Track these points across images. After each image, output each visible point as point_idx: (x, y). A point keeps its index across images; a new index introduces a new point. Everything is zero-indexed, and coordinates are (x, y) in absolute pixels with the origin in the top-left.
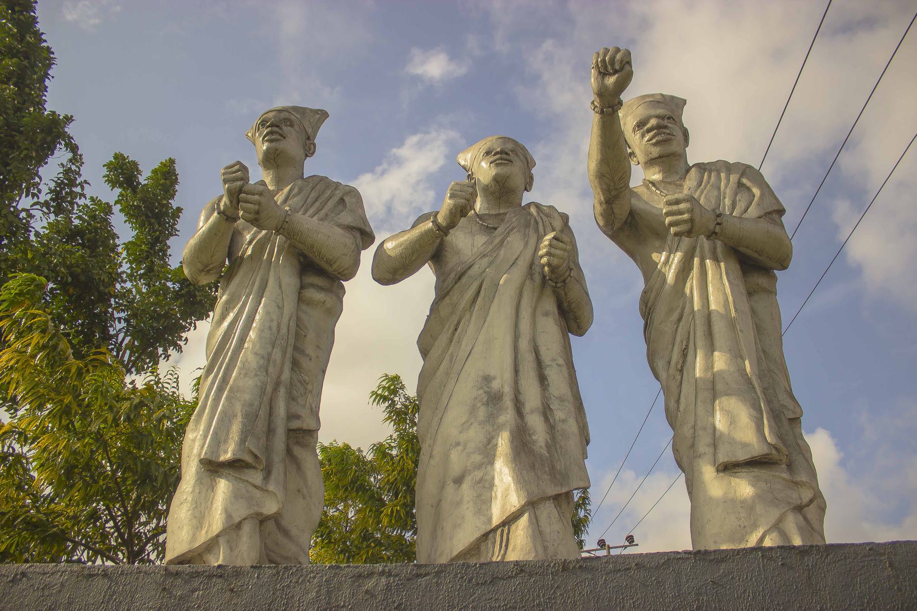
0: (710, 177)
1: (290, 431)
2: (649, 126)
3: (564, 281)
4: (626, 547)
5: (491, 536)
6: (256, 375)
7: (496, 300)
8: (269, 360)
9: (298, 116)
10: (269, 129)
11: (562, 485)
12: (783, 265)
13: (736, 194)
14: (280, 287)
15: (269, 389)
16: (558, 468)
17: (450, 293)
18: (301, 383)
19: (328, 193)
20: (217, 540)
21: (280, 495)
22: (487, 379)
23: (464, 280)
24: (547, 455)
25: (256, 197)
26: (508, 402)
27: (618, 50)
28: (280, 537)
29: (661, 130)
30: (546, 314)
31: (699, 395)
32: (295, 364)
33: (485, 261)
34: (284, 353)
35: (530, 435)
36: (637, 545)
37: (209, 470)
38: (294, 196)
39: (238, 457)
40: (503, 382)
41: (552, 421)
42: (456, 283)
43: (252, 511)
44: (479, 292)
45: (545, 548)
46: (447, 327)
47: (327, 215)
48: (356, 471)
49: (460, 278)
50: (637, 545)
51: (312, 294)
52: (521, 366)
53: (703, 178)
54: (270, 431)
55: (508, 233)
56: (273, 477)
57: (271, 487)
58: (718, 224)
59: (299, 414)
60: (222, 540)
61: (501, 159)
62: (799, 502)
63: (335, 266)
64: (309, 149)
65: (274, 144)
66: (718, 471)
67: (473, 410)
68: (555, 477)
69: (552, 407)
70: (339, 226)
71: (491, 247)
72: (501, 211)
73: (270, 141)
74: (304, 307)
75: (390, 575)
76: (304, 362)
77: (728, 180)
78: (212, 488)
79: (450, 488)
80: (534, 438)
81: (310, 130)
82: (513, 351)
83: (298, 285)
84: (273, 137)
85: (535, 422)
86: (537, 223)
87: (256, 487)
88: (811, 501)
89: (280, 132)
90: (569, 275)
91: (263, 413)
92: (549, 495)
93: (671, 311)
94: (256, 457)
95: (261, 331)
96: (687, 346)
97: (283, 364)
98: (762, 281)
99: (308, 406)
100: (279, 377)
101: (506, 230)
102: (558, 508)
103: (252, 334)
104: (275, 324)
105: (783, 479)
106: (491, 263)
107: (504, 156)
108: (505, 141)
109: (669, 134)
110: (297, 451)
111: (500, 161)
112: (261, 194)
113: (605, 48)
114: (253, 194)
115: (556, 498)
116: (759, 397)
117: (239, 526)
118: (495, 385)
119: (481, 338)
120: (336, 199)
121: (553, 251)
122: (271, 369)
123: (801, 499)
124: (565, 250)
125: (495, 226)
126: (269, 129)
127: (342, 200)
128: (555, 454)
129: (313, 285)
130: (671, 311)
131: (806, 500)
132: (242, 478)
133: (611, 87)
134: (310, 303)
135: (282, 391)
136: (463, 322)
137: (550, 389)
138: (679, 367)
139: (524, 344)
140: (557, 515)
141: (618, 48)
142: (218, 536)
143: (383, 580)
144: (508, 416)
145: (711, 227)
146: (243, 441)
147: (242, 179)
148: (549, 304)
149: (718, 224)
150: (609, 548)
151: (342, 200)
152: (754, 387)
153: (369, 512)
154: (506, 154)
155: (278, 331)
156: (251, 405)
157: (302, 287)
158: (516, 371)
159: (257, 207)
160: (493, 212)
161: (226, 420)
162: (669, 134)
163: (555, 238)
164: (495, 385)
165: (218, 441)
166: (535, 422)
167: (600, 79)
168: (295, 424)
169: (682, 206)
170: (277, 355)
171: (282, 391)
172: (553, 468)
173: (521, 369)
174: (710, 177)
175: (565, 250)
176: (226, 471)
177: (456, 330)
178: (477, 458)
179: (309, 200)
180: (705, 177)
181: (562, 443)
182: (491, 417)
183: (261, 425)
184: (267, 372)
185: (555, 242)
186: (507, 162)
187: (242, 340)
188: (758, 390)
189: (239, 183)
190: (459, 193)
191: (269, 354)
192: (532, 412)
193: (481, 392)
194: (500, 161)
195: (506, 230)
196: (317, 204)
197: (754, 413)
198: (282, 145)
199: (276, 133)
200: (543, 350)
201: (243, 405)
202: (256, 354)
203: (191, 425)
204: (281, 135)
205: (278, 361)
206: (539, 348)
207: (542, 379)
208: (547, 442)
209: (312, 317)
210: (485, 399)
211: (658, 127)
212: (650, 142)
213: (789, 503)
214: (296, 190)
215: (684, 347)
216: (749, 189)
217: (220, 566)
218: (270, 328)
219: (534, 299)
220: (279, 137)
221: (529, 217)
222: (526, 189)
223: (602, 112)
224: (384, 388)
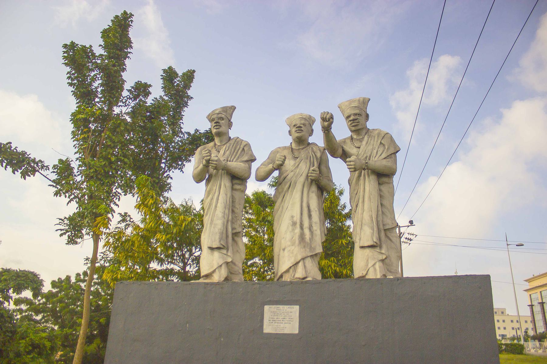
0: (371, 140)
1: (233, 234)
2: (350, 119)
3: (318, 181)
4: (408, 226)
5: (292, 267)
6: (221, 219)
7: (295, 190)
8: (224, 214)
9: (225, 114)
10: (215, 124)
11: (313, 252)
12: (393, 173)
13: (378, 148)
14: (226, 187)
15: (225, 223)
16: (313, 246)
17: (282, 184)
18: (235, 217)
19: (238, 147)
20: (215, 271)
21: (232, 256)
22: (292, 217)
23: (286, 180)
24: (309, 242)
25: (215, 162)
26: (298, 225)
27: (328, 113)
28: (233, 266)
29: (354, 121)
30: (313, 192)
31: (358, 222)
32: (233, 211)
33: (292, 173)
34: (229, 210)
35: (305, 236)
36: (415, 225)
37: (210, 249)
38: (227, 150)
39: (219, 246)
40: (297, 218)
41: (312, 230)
42: (283, 180)
43: (224, 262)
44: (290, 185)
45: (306, 271)
46: (281, 195)
47: (238, 157)
48: (264, 215)
49: (284, 179)
50: (415, 225)
52: (303, 213)
53: (368, 139)
54: (227, 237)
55: (301, 162)
56: (229, 251)
57: (229, 254)
58: (366, 166)
59: (235, 227)
60: (217, 270)
61: (299, 130)
62: (381, 259)
63: (243, 177)
64: (230, 125)
65: (217, 130)
66: (360, 248)
67: (288, 228)
68: (311, 250)
69: (313, 226)
70: (243, 162)
71: (294, 168)
72: (300, 148)
73: (216, 129)
74: (234, 192)
75: (260, 284)
76: (236, 210)
77: (377, 141)
78: (212, 255)
79: (282, 251)
80: (306, 237)
81: (229, 118)
82: (300, 208)
83: (231, 184)
84: (217, 127)
86: (310, 157)
87: (224, 254)
88: (386, 258)
89: (219, 125)
90: (320, 179)
91: (224, 232)
92: (309, 256)
93: (354, 190)
94: (223, 246)
95: (221, 203)
96: (358, 204)
97: (229, 214)
98: (385, 179)
99: (238, 224)
100: (228, 218)
101: (300, 160)
102: (312, 259)
103: (219, 205)
104: (225, 201)
105: (378, 252)
106: (294, 174)
107: (299, 129)
108: (301, 119)
109: (357, 122)
110: (236, 238)
111: (298, 131)
112: (216, 161)
114: (214, 161)
115: (311, 256)
116: (374, 225)
117: (221, 266)
118: (295, 219)
119: (291, 202)
120: (241, 149)
121: (312, 175)
122: (225, 216)
123: (382, 258)
124: (316, 174)
125: (297, 157)
126: (215, 124)
127: (243, 149)
128: (312, 242)
129: (236, 184)
130: (354, 190)
131: (384, 258)
132: (220, 252)
133: (326, 126)
134: (236, 190)
135: (230, 223)
136: (285, 195)
137: (312, 219)
138: (355, 210)
139: (305, 205)
140: (311, 261)
141: (328, 112)
142: (215, 269)
143: (258, 285)
144: (298, 230)
145: (364, 167)
146: (220, 241)
147: (209, 156)
148: (314, 188)
149: (367, 166)
150: (400, 227)
151: (243, 149)
152: (373, 222)
153: (270, 231)
154: (301, 127)
155: (226, 203)
156: (221, 229)
157: (233, 185)
158: (302, 214)
159: (215, 165)
160: (298, 148)
162: (357, 122)
163: (313, 170)
164: (295, 219)
167: (323, 123)
168: (234, 231)
169: (352, 163)
170: (227, 211)
171: (230, 223)
172: (311, 246)
173: (303, 214)
174: (371, 140)
175: (316, 174)
176: (216, 250)
177: (284, 197)
178: (289, 243)
179: (232, 152)
180: (370, 140)
181: (315, 238)
182: (293, 230)
183: (224, 236)
184: (224, 218)
185: (312, 172)
186: (300, 131)
187: (216, 207)
188: (374, 223)
189: (209, 157)
190: (280, 159)
191: (225, 211)
192: (306, 228)
193: (290, 221)
194: (298, 131)
195: (300, 160)
196: (235, 153)
197: (371, 231)
198: (220, 130)
199: (218, 125)
200: (311, 205)
201: (219, 230)
202: (221, 212)
203: (202, 234)
204: (220, 126)
205: (227, 213)
206: (310, 205)
207: (310, 216)
208: (310, 238)
210: (291, 224)
211: (353, 120)
212: (351, 125)
213: (378, 259)
214: (227, 148)
215: (357, 204)
216: (384, 145)
217: (218, 282)
218: (224, 202)
219: (308, 188)
220: (219, 127)
221: (308, 154)
222: (310, 136)
223: (324, 132)
224: (273, 182)
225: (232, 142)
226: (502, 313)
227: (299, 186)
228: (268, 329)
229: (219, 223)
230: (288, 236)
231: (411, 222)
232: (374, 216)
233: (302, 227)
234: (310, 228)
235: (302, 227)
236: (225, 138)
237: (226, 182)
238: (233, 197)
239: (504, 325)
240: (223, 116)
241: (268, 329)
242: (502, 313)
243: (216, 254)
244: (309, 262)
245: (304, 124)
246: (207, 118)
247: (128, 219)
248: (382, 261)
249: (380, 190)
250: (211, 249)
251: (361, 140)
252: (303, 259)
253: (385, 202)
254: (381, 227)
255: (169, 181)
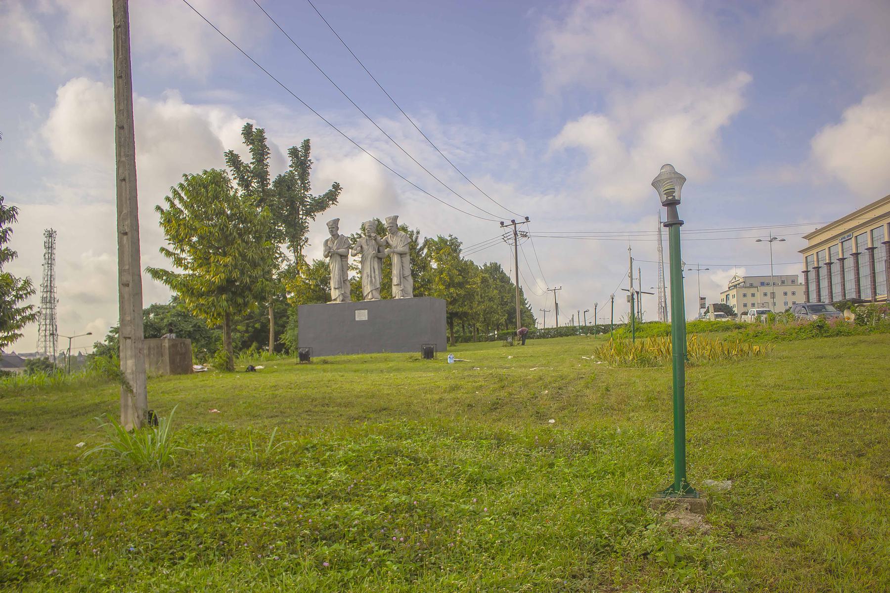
40: (369, 273)
51: (344, 260)
85: (373, 279)
98: (404, 255)
113: (378, 220)
150: (516, 224)
161: (335, 282)
165: (335, 285)
166: (373, 279)
207: (374, 272)
209: (344, 263)
225: (339, 238)
226: (793, 282)
227: (369, 259)
228: (357, 319)
229: (337, 277)
230: (366, 281)
231: (527, 218)
232: (398, 272)
233: (371, 277)
234: (375, 277)
235: (371, 277)
236: (336, 236)
237: (338, 258)
238: (342, 265)
239: (753, 300)
240: (333, 226)
241: (357, 319)
242: (793, 282)
243: (337, 291)
244: (374, 292)
245: (371, 229)
246: (327, 224)
247: (283, 255)
248: (401, 290)
249: (402, 260)
250: (335, 288)
251: (393, 238)
252: (371, 291)
253: (404, 265)
254: (402, 276)
255: (307, 224)
